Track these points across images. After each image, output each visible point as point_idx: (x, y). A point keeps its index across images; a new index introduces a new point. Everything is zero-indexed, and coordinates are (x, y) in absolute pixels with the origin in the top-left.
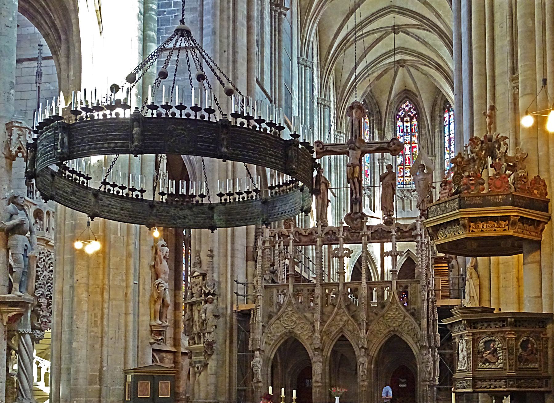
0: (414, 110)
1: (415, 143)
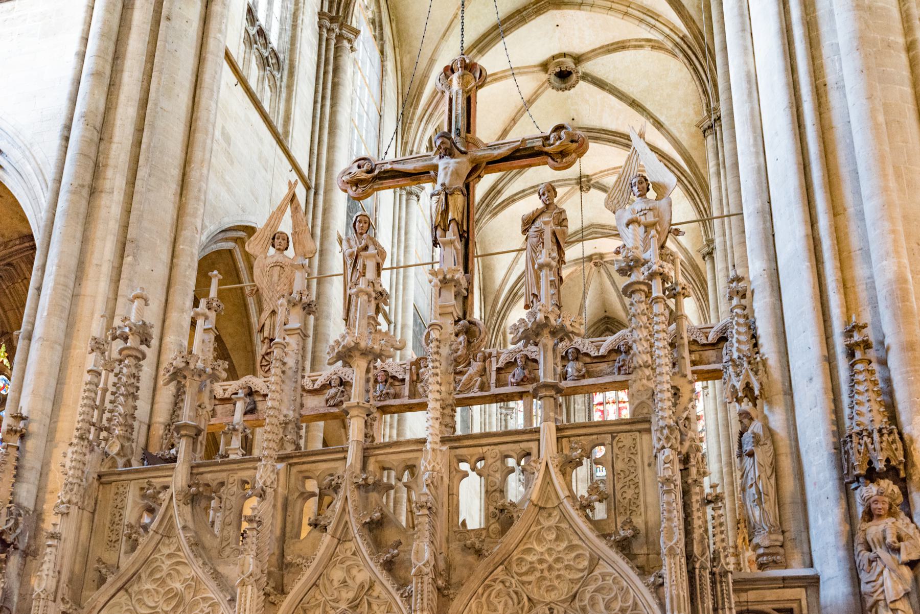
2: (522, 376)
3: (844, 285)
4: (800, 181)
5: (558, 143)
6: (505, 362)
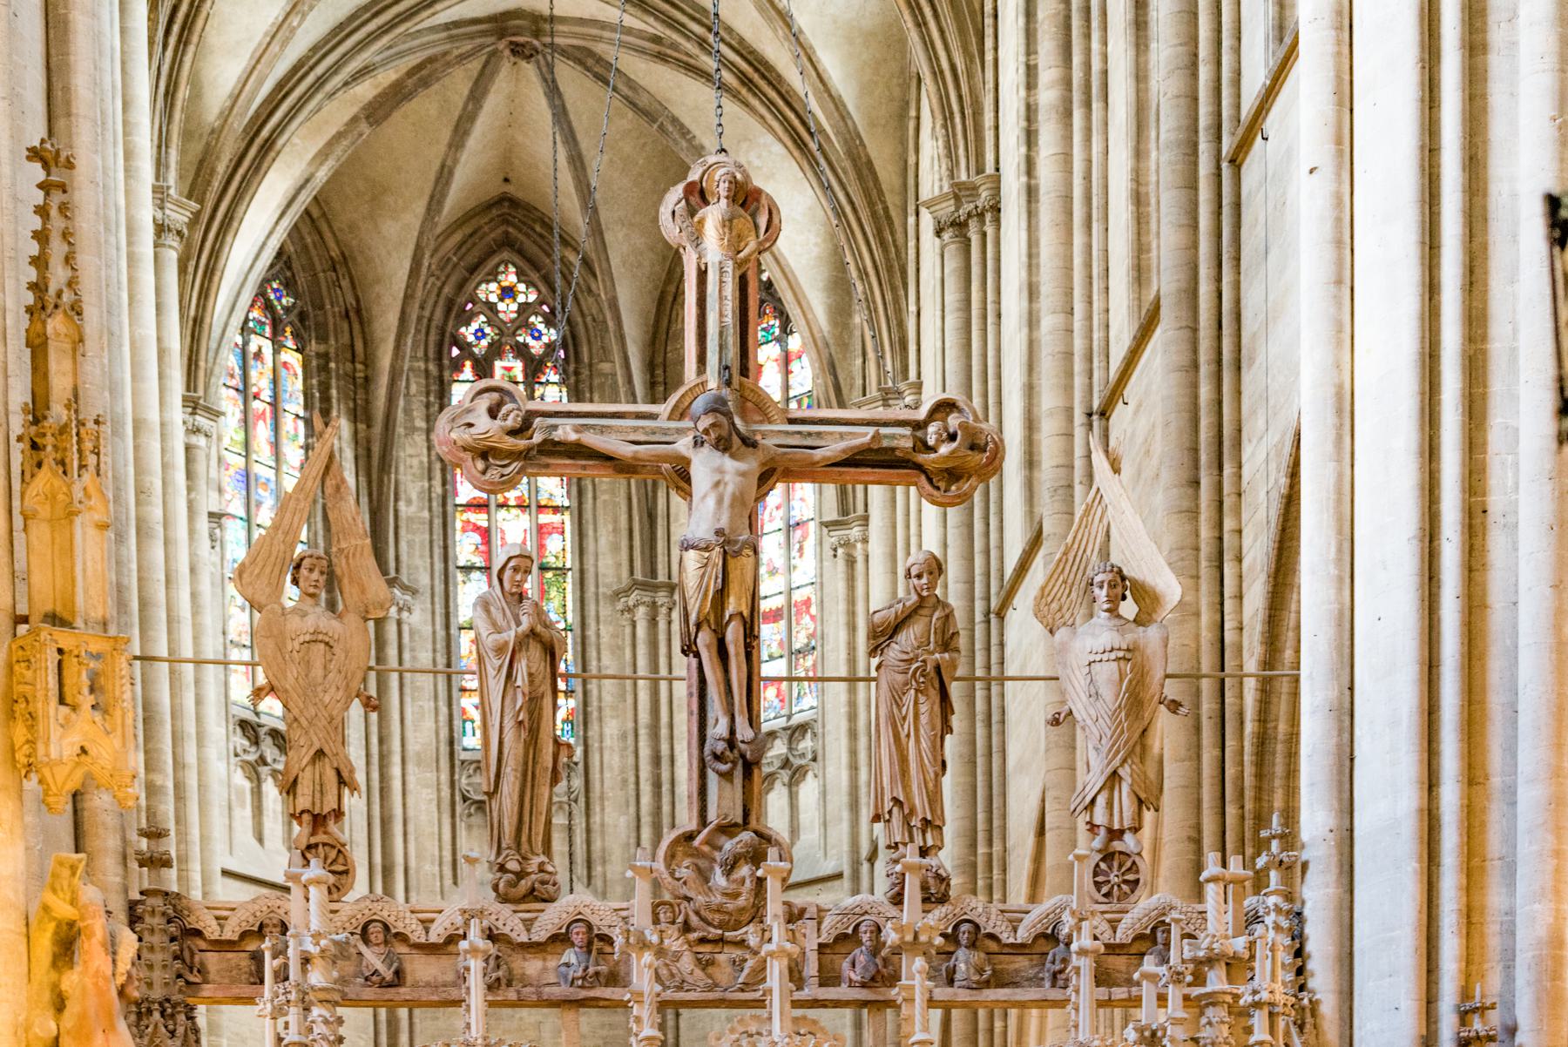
0: (549, 322)
1: (556, 509)
2: (872, 970)
3: (1468, 917)
4: (1421, 698)
5: (944, 449)
6: (834, 933)
